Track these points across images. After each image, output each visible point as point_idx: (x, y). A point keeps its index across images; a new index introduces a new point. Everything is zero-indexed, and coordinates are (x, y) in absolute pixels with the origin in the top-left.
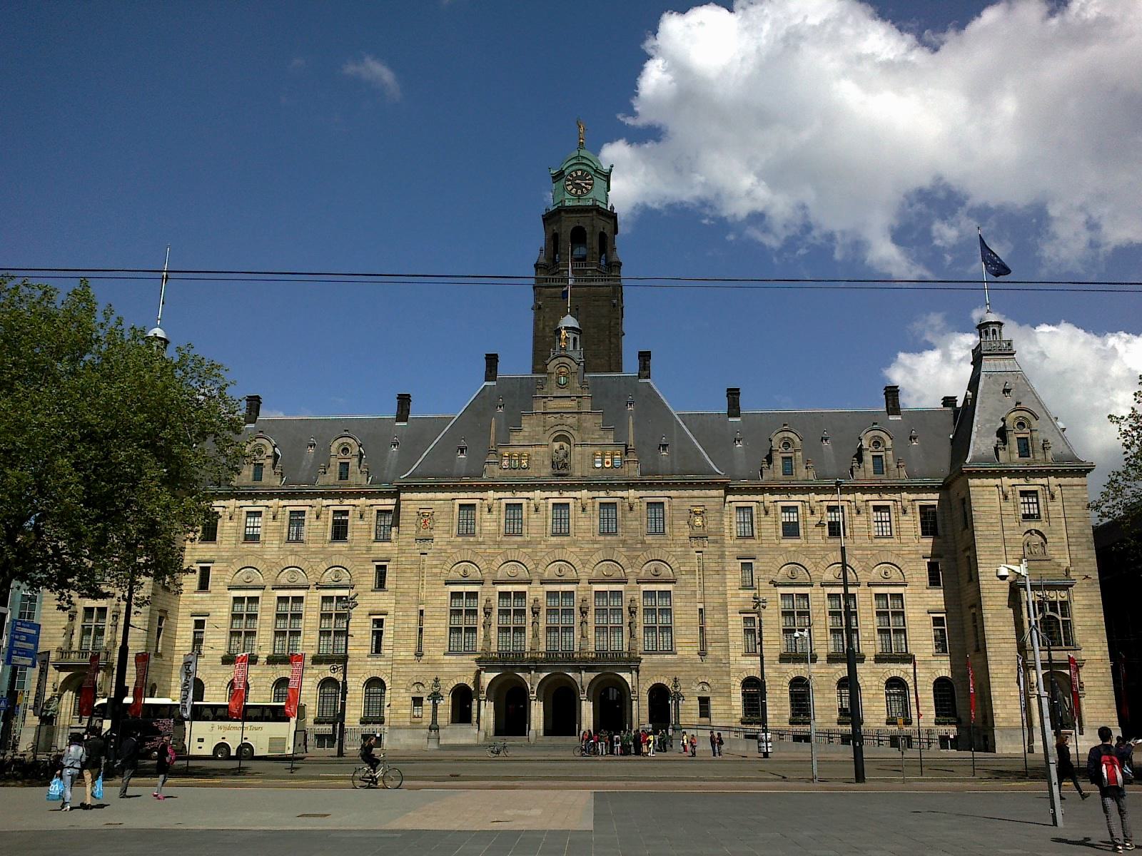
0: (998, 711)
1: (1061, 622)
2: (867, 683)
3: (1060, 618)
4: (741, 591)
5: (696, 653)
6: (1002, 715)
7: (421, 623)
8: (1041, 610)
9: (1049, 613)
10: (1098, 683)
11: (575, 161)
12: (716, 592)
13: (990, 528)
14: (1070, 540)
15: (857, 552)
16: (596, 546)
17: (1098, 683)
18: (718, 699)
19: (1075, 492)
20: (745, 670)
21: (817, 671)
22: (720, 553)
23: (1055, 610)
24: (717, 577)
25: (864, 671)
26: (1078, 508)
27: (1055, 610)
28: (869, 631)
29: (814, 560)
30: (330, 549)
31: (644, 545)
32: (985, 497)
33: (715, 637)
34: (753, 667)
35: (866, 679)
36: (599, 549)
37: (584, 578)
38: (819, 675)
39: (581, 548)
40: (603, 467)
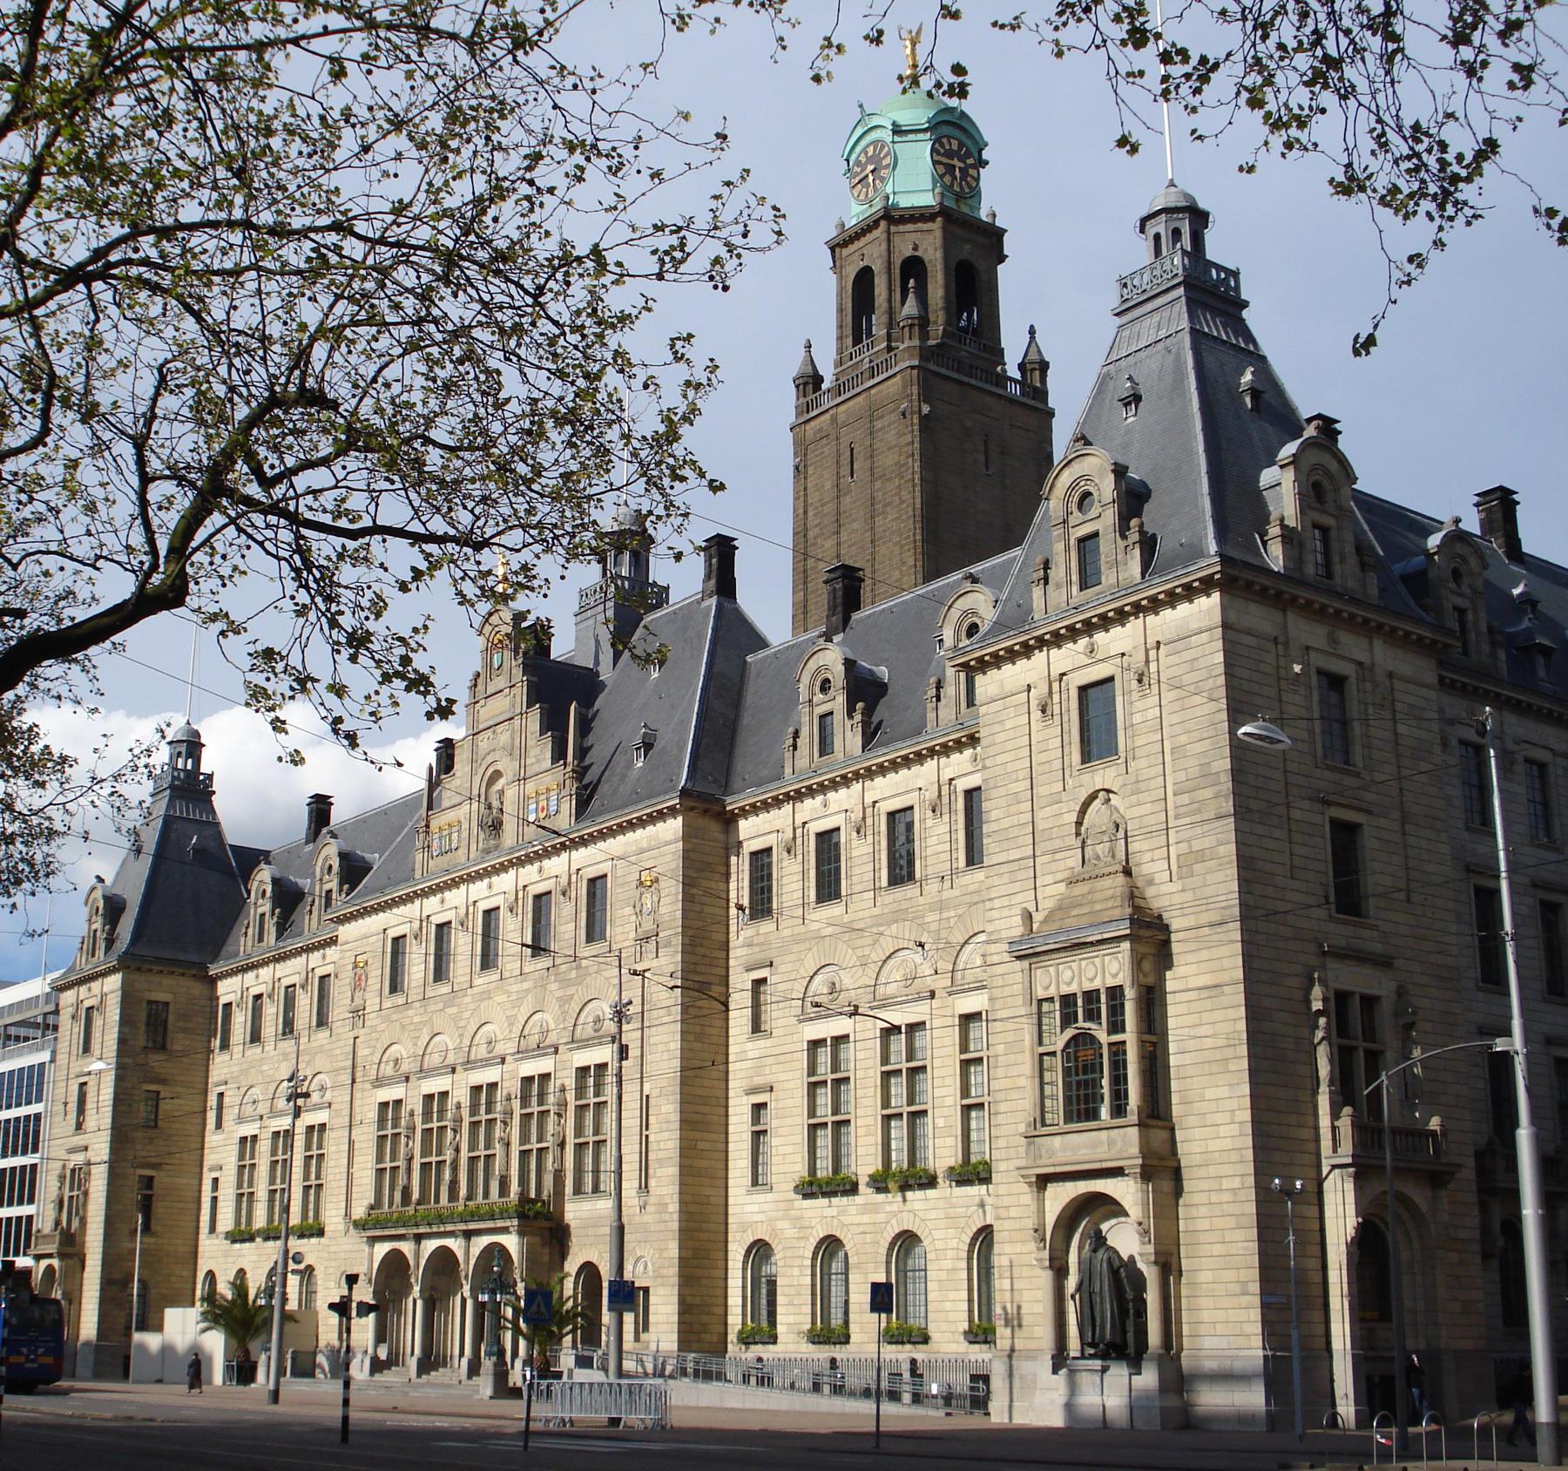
2: (939, 1244)
4: (750, 1045)
8: (1068, 1019)
10: (1220, 1223)
11: (859, 131)
12: (665, 1056)
13: (1014, 809)
16: (526, 985)
17: (1220, 1223)
20: (751, 1224)
21: (857, 1219)
23: (1092, 1015)
25: (933, 1215)
26: (1198, 699)
27: (1092, 1015)
28: (945, 1112)
29: (859, 952)
30: (314, 1044)
31: (581, 972)
32: (1009, 724)
34: (760, 1217)
35: (937, 1234)
36: (528, 991)
37: (510, 1047)
38: (861, 1229)
39: (509, 993)
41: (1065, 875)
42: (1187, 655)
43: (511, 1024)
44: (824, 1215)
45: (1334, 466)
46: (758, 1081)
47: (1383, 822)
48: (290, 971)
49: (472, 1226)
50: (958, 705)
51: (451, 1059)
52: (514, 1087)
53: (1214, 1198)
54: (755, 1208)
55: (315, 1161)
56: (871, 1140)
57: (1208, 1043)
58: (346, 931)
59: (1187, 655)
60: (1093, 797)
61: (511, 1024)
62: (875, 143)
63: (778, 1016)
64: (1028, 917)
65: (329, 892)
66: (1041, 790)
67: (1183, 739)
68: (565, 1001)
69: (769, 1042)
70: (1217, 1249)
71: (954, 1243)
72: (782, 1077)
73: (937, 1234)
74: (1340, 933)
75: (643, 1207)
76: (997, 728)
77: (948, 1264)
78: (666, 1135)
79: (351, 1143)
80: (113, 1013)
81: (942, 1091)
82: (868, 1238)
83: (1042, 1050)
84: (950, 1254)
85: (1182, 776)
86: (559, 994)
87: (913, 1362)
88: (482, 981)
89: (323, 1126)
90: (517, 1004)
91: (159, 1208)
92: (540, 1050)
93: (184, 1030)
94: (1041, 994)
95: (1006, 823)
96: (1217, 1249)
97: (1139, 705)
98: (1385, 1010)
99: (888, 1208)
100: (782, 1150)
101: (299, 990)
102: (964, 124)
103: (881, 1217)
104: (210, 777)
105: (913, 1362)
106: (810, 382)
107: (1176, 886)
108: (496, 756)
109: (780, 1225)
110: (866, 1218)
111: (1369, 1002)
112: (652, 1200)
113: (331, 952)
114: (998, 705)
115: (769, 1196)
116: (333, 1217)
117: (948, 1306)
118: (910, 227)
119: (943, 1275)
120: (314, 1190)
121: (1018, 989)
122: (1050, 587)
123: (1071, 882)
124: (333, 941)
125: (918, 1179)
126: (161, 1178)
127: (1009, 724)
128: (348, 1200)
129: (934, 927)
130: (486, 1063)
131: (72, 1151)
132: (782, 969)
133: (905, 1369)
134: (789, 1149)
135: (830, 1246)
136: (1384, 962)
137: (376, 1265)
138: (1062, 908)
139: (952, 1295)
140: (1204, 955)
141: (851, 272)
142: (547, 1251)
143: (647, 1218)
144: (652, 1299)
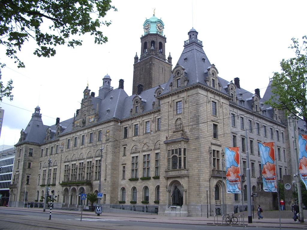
0: (161, 198)
1: (178, 158)
2: (151, 188)
3: (178, 156)
4: (123, 157)
5: (104, 180)
6: (162, 200)
7: (60, 174)
8: (173, 153)
9: (175, 154)
10: (195, 185)
12: (110, 159)
14: (191, 120)
15: (151, 138)
17: (195, 185)
18: (108, 195)
19: (194, 97)
21: (138, 184)
22: (111, 145)
23: (176, 153)
24: (110, 153)
27: (176, 153)
28: (153, 168)
32: (165, 108)
33: (108, 174)
35: (151, 187)
40: (91, 122)
41: (173, 131)
42: (193, 98)
43: (86, 153)
44: (133, 184)
45: (215, 71)
46: (124, 163)
47: (221, 125)
48: (52, 145)
49: (78, 184)
50: (157, 105)
51: (76, 159)
52: (86, 163)
53: (194, 181)
54: (123, 182)
55: (55, 174)
56: (141, 172)
57: (194, 157)
58: (61, 139)
59: (193, 98)
60: (178, 119)
61: (86, 153)
62: (148, 24)
63: (128, 153)
64: (167, 138)
65: (59, 132)
66: (170, 118)
67: (192, 110)
68: (94, 150)
69: (126, 157)
70: (194, 189)
71: (153, 188)
72: (127, 162)
73: (151, 187)
74: (214, 141)
75: (105, 182)
76: (163, 108)
77: (152, 191)
78: (109, 171)
79: (60, 171)
80: (24, 150)
81: (152, 165)
82: (140, 187)
83: (168, 158)
84: (153, 190)
85: (191, 116)
86: (93, 149)
87: (146, 206)
88: (81, 147)
89: (56, 169)
90: (87, 150)
91: (30, 181)
92: (90, 158)
93: (35, 153)
94: (168, 149)
95: (164, 123)
96: (194, 189)
97: (185, 105)
98: (221, 152)
99: (143, 183)
100: (127, 173)
101: (53, 148)
102: (161, 22)
103: (142, 184)
104: (41, 114)
105: (146, 206)
106: (136, 58)
107: (190, 133)
108: (85, 111)
109: (126, 185)
110: (140, 184)
111: (218, 152)
112: (107, 181)
113: (59, 142)
114: (164, 105)
115: (125, 181)
116: (57, 183)
117: (152, 198)
118: (153, 36)
119: (151, 193)
120: (55, 178)
121: (165, 149)
122: (172, 87)
123: (174, 132)
124: (58, 140)
125: (148, 178)
126: (30, 176)
127: (165, 108)
128: (60, 180)
129: (152, 139)
130: (82, 159)
131: (17, 172)
132: (128, 146)
133: (145, 207)
134: (128, 173)
135: (134, 189)
136: (220, 146)
137: (63, 190)
138: (172, 136)
139: (153, 196)
140: (194, 144)
141: (144, 42)
142: (90, 188)
143: (106, 184)
144: (106, 196)
